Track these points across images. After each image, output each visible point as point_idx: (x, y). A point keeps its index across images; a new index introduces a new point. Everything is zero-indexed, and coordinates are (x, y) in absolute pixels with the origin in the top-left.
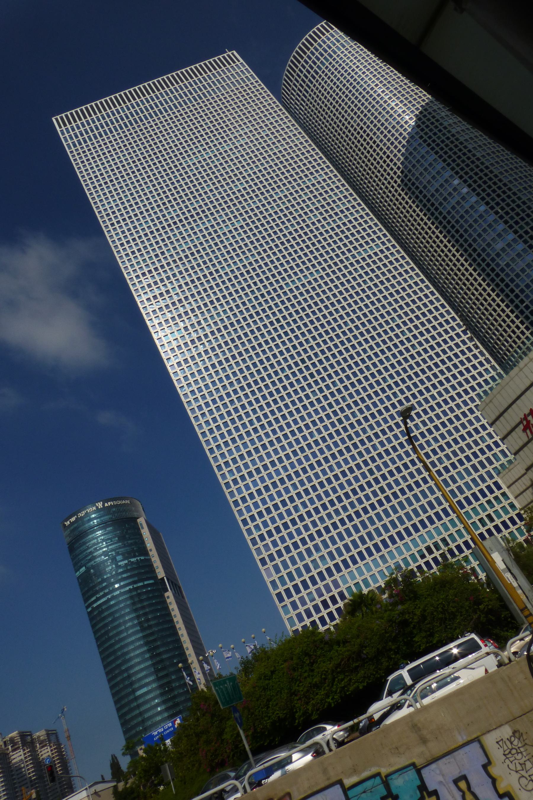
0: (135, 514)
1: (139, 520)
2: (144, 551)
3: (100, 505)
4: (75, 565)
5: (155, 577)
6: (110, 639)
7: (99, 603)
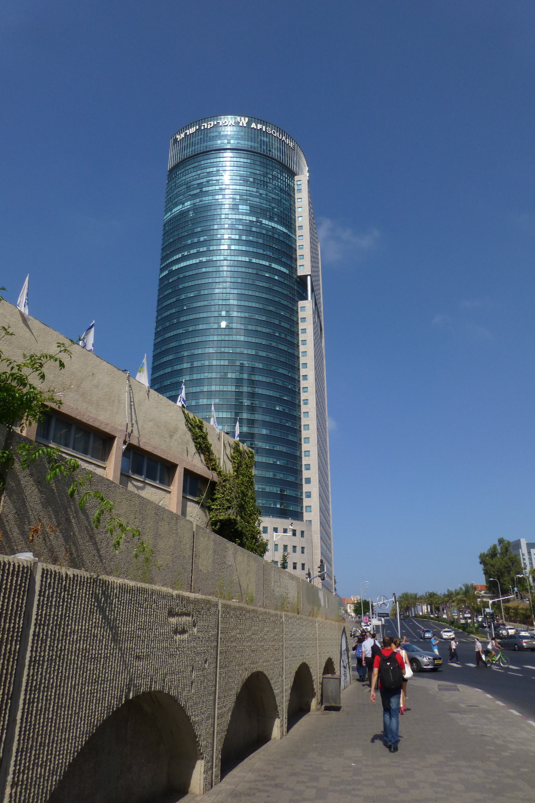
0: (295, 169)
1: (296, 178)
2: (288, 218)
3: (244, 121)
5: (293, 269)
6: (180, 324)
7: (182, 264)
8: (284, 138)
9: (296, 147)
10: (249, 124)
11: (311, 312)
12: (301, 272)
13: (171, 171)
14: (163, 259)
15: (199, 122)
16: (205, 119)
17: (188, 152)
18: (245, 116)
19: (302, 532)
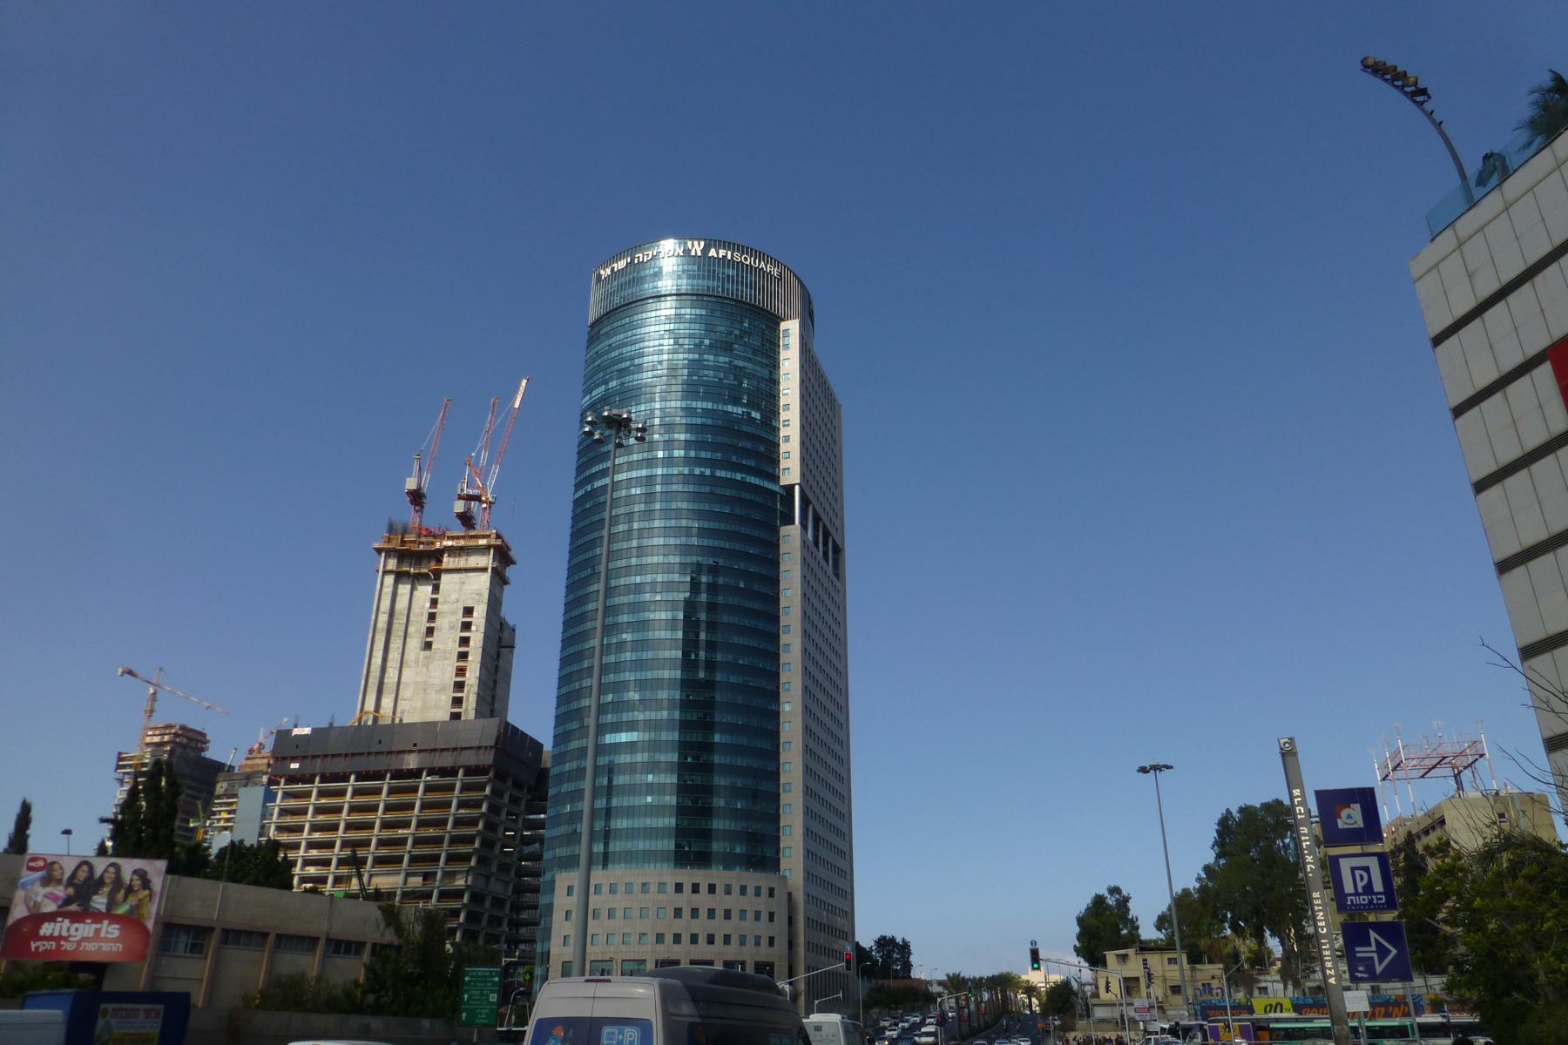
0: (781, 309)
1: (783, 325)
3: (697, 248)
4: (587, 377)
8: (762, 265)
9: (786, 273)
10: (705, 250)
11: (798, 544)
12: (784, 481)
13: (593, 325)
14: (580, 469)
15: (632, 250)
16: (639, 247)
17: (617, 301)
18: (699, 240)
19: (771, 893)
